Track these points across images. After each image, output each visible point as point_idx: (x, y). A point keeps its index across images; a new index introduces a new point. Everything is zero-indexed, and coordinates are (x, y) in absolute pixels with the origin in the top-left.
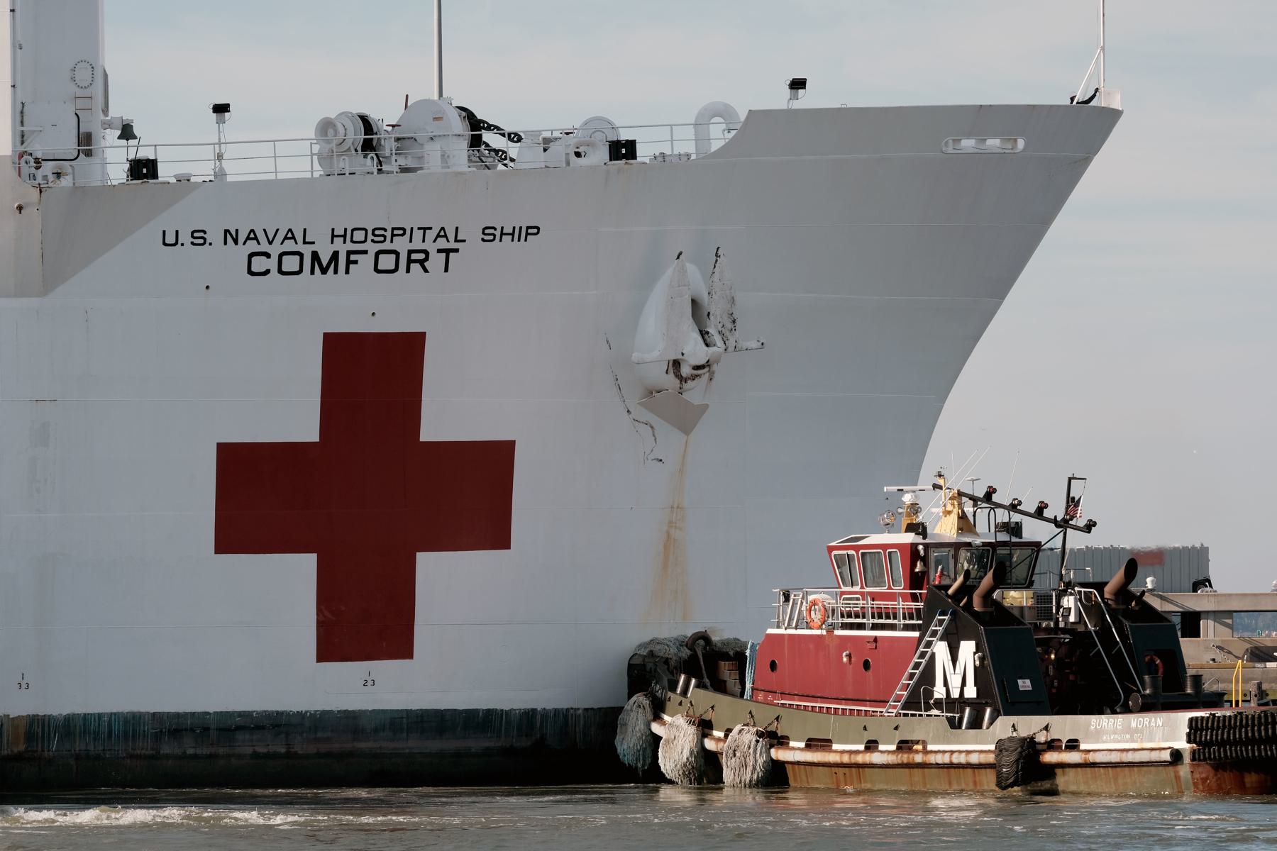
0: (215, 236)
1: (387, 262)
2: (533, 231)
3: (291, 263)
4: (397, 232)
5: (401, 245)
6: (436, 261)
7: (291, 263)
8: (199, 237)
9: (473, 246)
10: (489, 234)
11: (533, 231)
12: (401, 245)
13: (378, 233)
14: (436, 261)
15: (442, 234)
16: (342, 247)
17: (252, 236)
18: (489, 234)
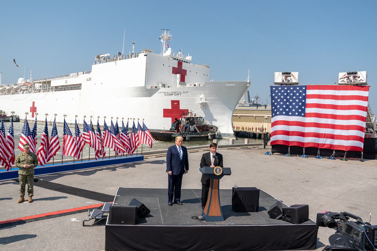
0: (162, 92)
1: (175, 95)
2: (187, 92)
3: (168, 95)
4: (176, 92)
5: (176, 93)
6: (179, 94)
7: (168, 95)
8: (161, 93)
9: (182, 94)
10: (184, 92)
11: (187, 92)
12: (176, 93)
13: (174, 92)
14: (179, 94)
15: (180, 92)
16: (172, 93)
17: (165, 92)
18: (184, 92)
